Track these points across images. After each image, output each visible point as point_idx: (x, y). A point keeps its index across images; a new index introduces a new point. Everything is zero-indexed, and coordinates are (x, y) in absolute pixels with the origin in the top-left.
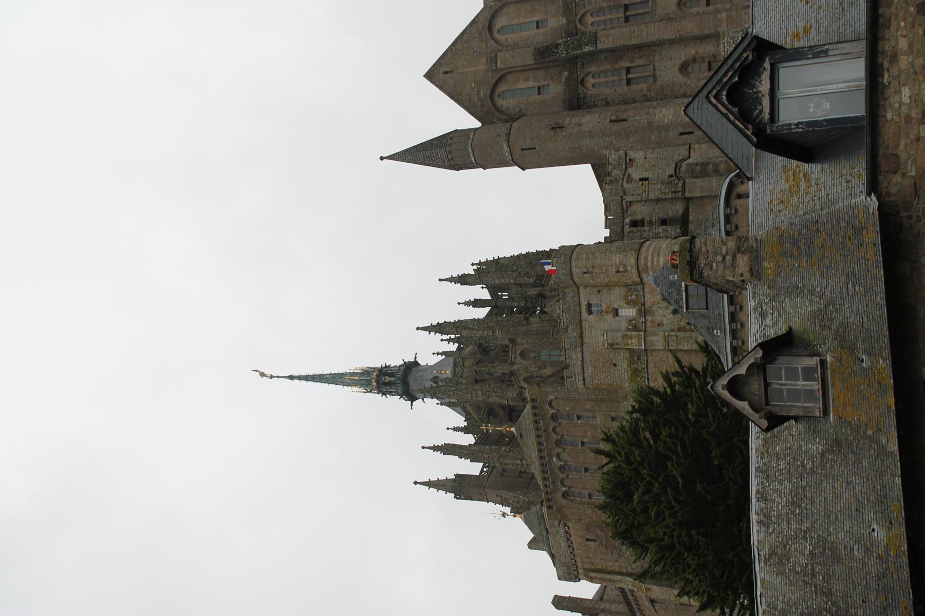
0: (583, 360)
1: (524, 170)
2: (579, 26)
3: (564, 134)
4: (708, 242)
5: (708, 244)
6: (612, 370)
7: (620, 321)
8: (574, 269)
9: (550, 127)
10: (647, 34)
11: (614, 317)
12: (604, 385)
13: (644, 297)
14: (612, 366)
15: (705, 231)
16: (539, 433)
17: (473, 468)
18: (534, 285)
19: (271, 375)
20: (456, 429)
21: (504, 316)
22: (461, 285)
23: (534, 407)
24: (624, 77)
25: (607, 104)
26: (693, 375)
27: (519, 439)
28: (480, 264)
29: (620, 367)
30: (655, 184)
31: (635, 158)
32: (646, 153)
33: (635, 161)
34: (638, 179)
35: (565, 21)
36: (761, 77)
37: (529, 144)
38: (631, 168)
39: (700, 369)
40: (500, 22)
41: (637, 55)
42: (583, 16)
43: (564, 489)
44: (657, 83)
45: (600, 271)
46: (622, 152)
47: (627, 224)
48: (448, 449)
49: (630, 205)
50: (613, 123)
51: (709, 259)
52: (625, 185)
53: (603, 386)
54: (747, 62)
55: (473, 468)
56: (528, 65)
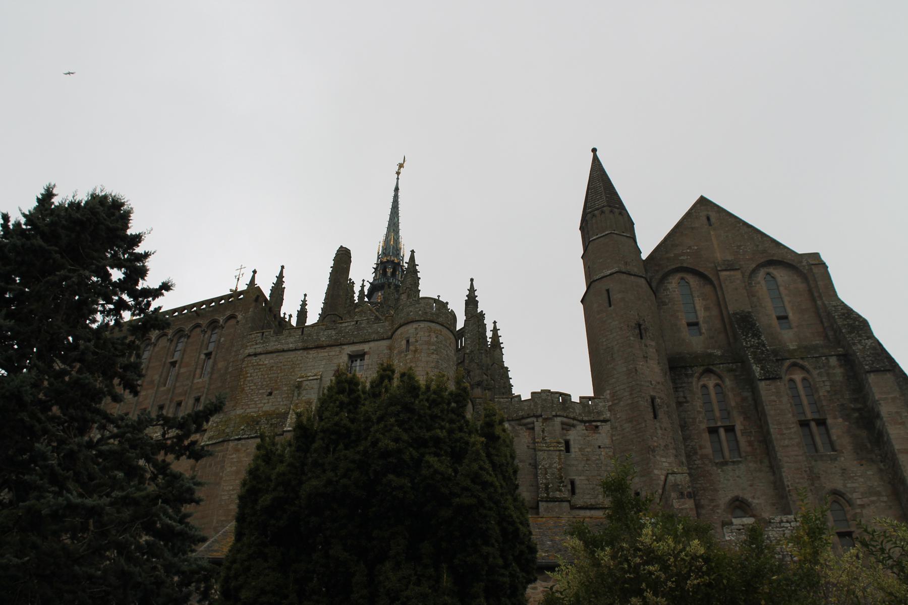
0: (284, 351)
2: (787, 363)
3: (632, 338)
6: (263, 391)
8: (415, 325)
9: (641, 322)
10: (787, 446)
14: (269, 391)
19: (400, 173)
22: (466, 300)
24: (719, 424)
25: (679, 404)
29: (266, 401)
30: (560, 459)
31: (600, 433)
32: (607, 448)
33: (595, 433)
34: (568, 438)
35: (792, 348)
37: (615, 297)
38: (584, 428)
40: (781, 275)
41: (752, 439)
42: (802, 368)
44: (715, 468)
45: (408, 361)
46: (608, 415)
49: (529, 429)
50: (650, 400)
52: (559, 419)
53: (242, 380)
56: (726, 308)
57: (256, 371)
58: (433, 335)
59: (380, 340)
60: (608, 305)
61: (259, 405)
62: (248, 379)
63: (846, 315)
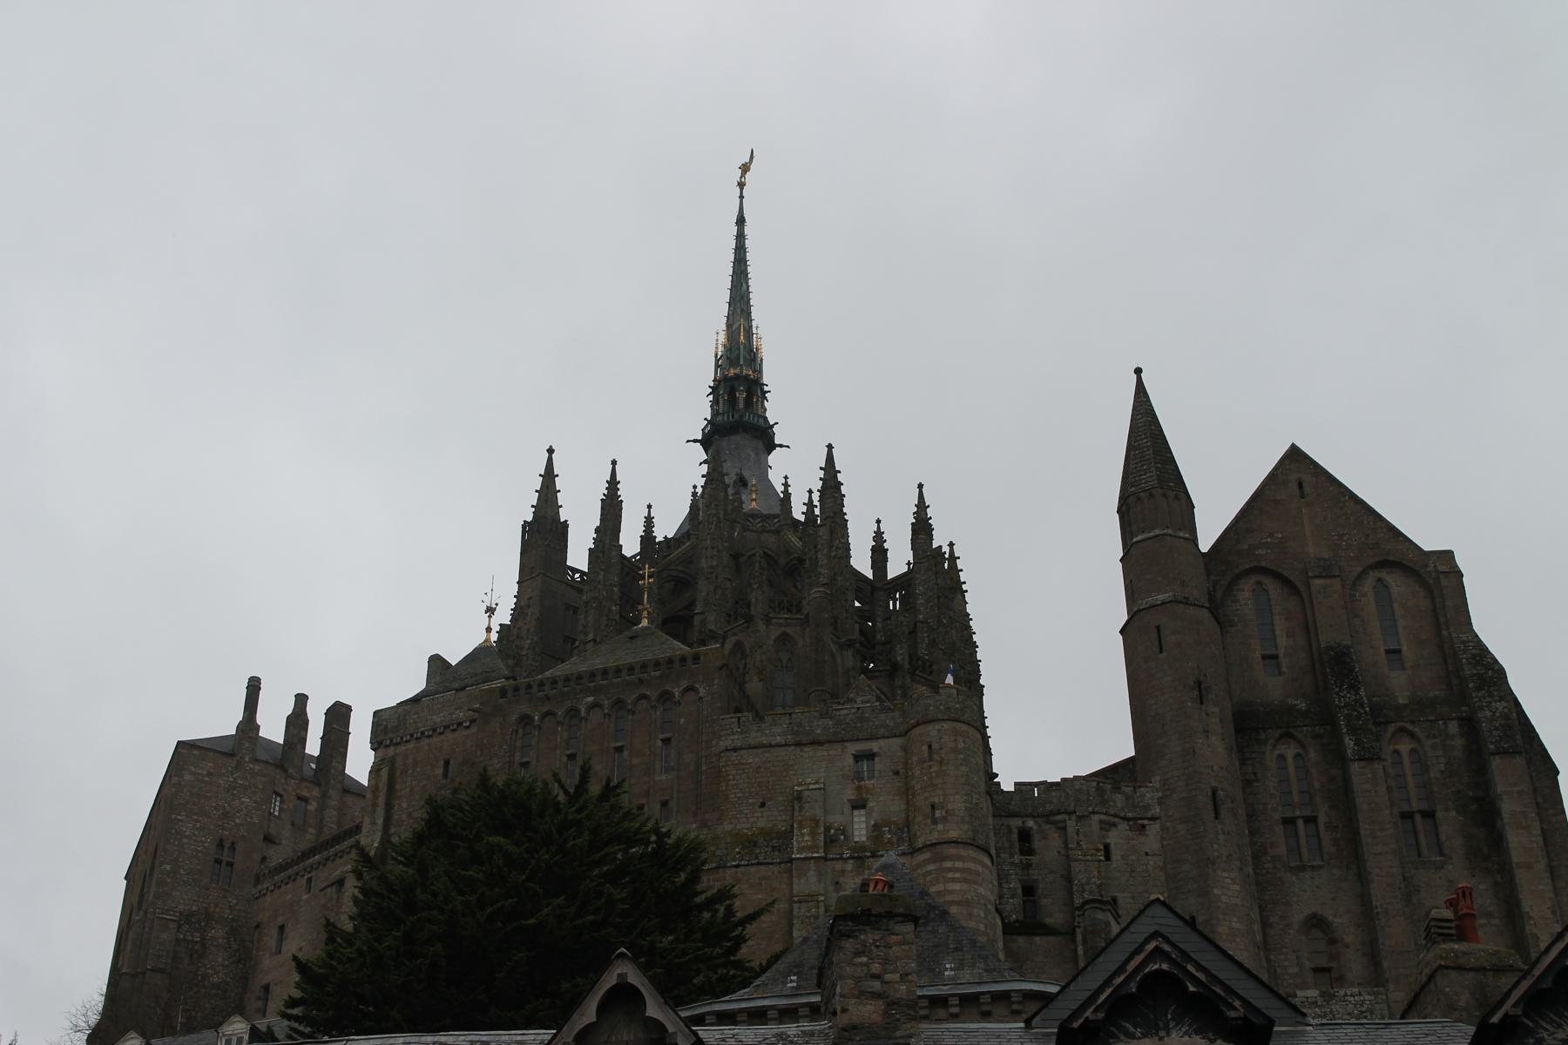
1: (1122, 632)
2: (1392, 728)
3: (1189, 704)
4: (907, 947)
5: (903, 947)
6: (754, 801)
7: (843, 813)
8: (937, 726)
9: (1202, 678)
10: (1380, 854)
11: (849, 801)
12: (727, 786)
14: (761, 800)
15: (980, 956)
17: (578, 556)
18: (913, 656)
20: (649, 522)
21: (857, 604)
23: (683, 659)
24: (1298, 813)
25: (1247, 783)
26: (729, 944)
27: (627, 634)
28: (953, 559)
29: (759, 815)
30: (1099, 872)
31: (1147, 835)
33: (1140, 834)
34: (1108, 841)
35: (1401, 701)
36: (1196, 1034)
38: (1128, 828)
39: (738, 957)
40: (1397, 584)
41: (1339, 836)
42: (1412, 735)
44: (1289, 874)
45: (934, 775)
46: (1158, 810)
47: (1023, 822)
48: (611, 507)
49: (1060, 828)
50: (1210, 794)
51: (875, 950)
52: (1096, 818)
54: (1224, 1009)
55: (578, 556)
57: (739, 772)
58: (960, 740)
59: (891, 737)
60: (1158, 650)
61: (752, 820)
62: (731, 782)
63: (1478, 658)
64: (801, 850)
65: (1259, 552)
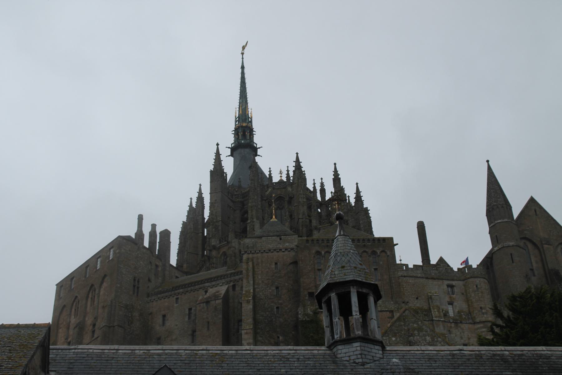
6: (414, 296)
8: (479, 279)
11: (448, 301)
13: (466, 323)
14: (416, 297)
16: (361, 241)
43: (323, 253)
60: (511, 262)
61: (415, 303)
64: (436, 317)
65: (525, 232)
